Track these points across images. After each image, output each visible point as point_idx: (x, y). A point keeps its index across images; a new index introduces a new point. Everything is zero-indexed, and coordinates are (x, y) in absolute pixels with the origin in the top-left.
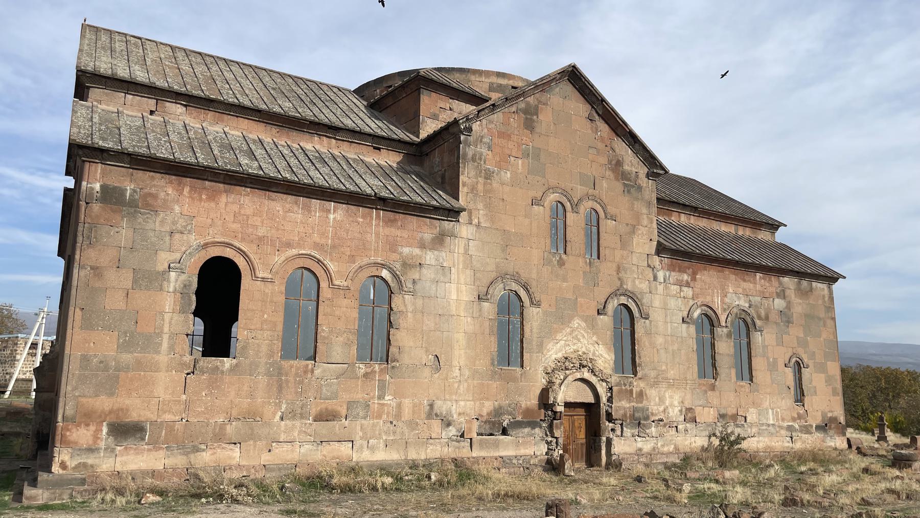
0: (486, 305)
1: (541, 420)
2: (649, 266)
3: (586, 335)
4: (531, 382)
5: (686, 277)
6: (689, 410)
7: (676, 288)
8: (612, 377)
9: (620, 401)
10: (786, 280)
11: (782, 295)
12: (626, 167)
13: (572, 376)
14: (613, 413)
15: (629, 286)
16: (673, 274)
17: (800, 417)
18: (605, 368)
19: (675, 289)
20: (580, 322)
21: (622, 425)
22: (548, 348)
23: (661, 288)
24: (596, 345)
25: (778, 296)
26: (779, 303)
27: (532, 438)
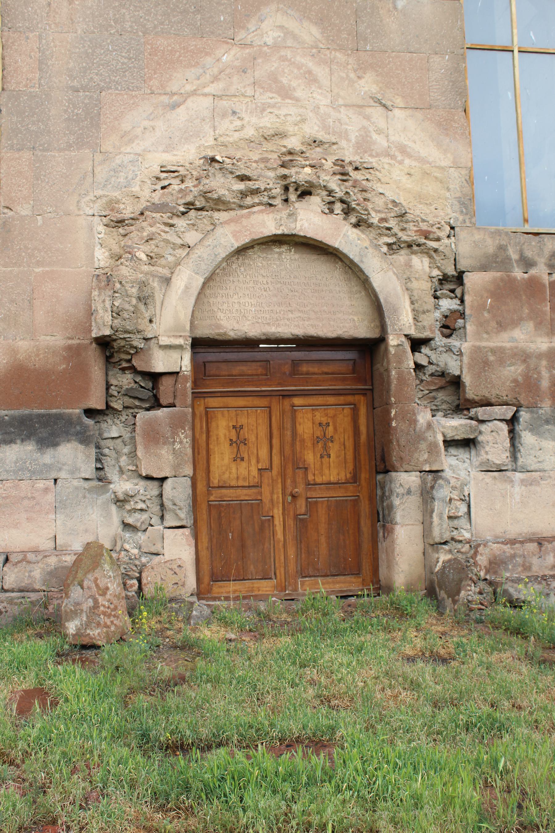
1: (90, 413)
3: (321, 72)
4: (38, 264)
8: (462, 233)
9: (502, 326)
13: (233, 227)
14: (467, 379)
18: (420, 198)
20: (292, 25)
21: (512, 422)
22: (126, 126)
24: (377, 113)
27: (41, 485)
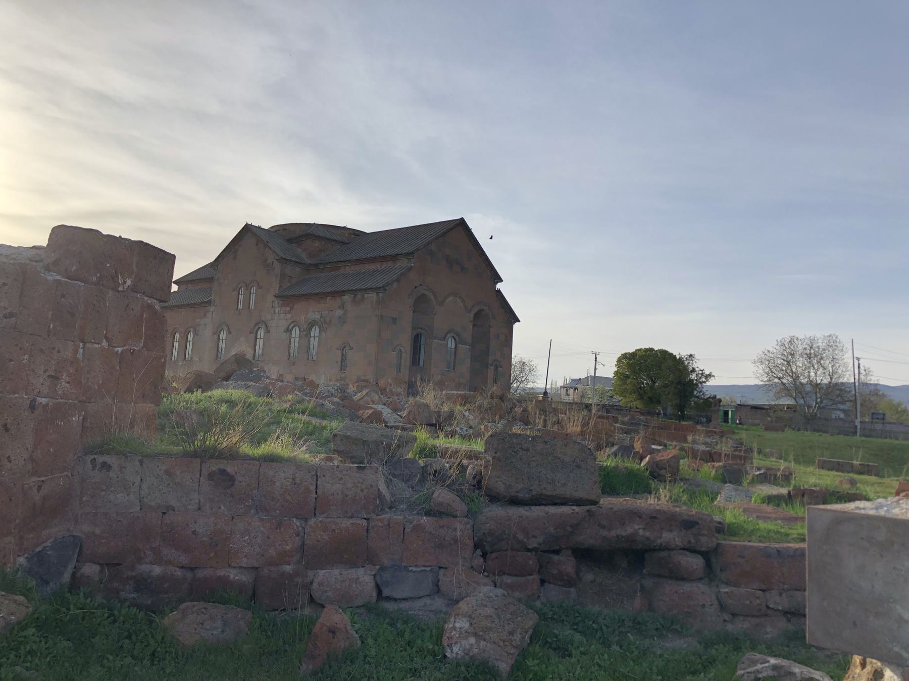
0: (215, 336)
2: (273, 307)
5: (288, 309)
6: (281, 375)
7: (283, 315)
10: (347, 298)
11: (342, 306)
12: (269, 261)
15: (263, 319)
16: (282, 308)
17: (341, 379)
19: (282, 316)
23: (276, 316)
25: (339, 308)
26: (339, 312)
